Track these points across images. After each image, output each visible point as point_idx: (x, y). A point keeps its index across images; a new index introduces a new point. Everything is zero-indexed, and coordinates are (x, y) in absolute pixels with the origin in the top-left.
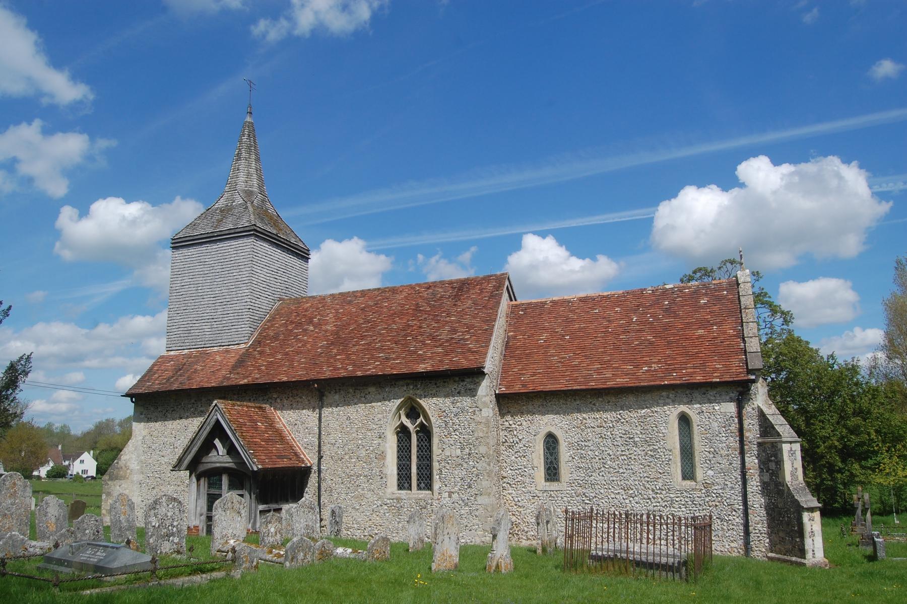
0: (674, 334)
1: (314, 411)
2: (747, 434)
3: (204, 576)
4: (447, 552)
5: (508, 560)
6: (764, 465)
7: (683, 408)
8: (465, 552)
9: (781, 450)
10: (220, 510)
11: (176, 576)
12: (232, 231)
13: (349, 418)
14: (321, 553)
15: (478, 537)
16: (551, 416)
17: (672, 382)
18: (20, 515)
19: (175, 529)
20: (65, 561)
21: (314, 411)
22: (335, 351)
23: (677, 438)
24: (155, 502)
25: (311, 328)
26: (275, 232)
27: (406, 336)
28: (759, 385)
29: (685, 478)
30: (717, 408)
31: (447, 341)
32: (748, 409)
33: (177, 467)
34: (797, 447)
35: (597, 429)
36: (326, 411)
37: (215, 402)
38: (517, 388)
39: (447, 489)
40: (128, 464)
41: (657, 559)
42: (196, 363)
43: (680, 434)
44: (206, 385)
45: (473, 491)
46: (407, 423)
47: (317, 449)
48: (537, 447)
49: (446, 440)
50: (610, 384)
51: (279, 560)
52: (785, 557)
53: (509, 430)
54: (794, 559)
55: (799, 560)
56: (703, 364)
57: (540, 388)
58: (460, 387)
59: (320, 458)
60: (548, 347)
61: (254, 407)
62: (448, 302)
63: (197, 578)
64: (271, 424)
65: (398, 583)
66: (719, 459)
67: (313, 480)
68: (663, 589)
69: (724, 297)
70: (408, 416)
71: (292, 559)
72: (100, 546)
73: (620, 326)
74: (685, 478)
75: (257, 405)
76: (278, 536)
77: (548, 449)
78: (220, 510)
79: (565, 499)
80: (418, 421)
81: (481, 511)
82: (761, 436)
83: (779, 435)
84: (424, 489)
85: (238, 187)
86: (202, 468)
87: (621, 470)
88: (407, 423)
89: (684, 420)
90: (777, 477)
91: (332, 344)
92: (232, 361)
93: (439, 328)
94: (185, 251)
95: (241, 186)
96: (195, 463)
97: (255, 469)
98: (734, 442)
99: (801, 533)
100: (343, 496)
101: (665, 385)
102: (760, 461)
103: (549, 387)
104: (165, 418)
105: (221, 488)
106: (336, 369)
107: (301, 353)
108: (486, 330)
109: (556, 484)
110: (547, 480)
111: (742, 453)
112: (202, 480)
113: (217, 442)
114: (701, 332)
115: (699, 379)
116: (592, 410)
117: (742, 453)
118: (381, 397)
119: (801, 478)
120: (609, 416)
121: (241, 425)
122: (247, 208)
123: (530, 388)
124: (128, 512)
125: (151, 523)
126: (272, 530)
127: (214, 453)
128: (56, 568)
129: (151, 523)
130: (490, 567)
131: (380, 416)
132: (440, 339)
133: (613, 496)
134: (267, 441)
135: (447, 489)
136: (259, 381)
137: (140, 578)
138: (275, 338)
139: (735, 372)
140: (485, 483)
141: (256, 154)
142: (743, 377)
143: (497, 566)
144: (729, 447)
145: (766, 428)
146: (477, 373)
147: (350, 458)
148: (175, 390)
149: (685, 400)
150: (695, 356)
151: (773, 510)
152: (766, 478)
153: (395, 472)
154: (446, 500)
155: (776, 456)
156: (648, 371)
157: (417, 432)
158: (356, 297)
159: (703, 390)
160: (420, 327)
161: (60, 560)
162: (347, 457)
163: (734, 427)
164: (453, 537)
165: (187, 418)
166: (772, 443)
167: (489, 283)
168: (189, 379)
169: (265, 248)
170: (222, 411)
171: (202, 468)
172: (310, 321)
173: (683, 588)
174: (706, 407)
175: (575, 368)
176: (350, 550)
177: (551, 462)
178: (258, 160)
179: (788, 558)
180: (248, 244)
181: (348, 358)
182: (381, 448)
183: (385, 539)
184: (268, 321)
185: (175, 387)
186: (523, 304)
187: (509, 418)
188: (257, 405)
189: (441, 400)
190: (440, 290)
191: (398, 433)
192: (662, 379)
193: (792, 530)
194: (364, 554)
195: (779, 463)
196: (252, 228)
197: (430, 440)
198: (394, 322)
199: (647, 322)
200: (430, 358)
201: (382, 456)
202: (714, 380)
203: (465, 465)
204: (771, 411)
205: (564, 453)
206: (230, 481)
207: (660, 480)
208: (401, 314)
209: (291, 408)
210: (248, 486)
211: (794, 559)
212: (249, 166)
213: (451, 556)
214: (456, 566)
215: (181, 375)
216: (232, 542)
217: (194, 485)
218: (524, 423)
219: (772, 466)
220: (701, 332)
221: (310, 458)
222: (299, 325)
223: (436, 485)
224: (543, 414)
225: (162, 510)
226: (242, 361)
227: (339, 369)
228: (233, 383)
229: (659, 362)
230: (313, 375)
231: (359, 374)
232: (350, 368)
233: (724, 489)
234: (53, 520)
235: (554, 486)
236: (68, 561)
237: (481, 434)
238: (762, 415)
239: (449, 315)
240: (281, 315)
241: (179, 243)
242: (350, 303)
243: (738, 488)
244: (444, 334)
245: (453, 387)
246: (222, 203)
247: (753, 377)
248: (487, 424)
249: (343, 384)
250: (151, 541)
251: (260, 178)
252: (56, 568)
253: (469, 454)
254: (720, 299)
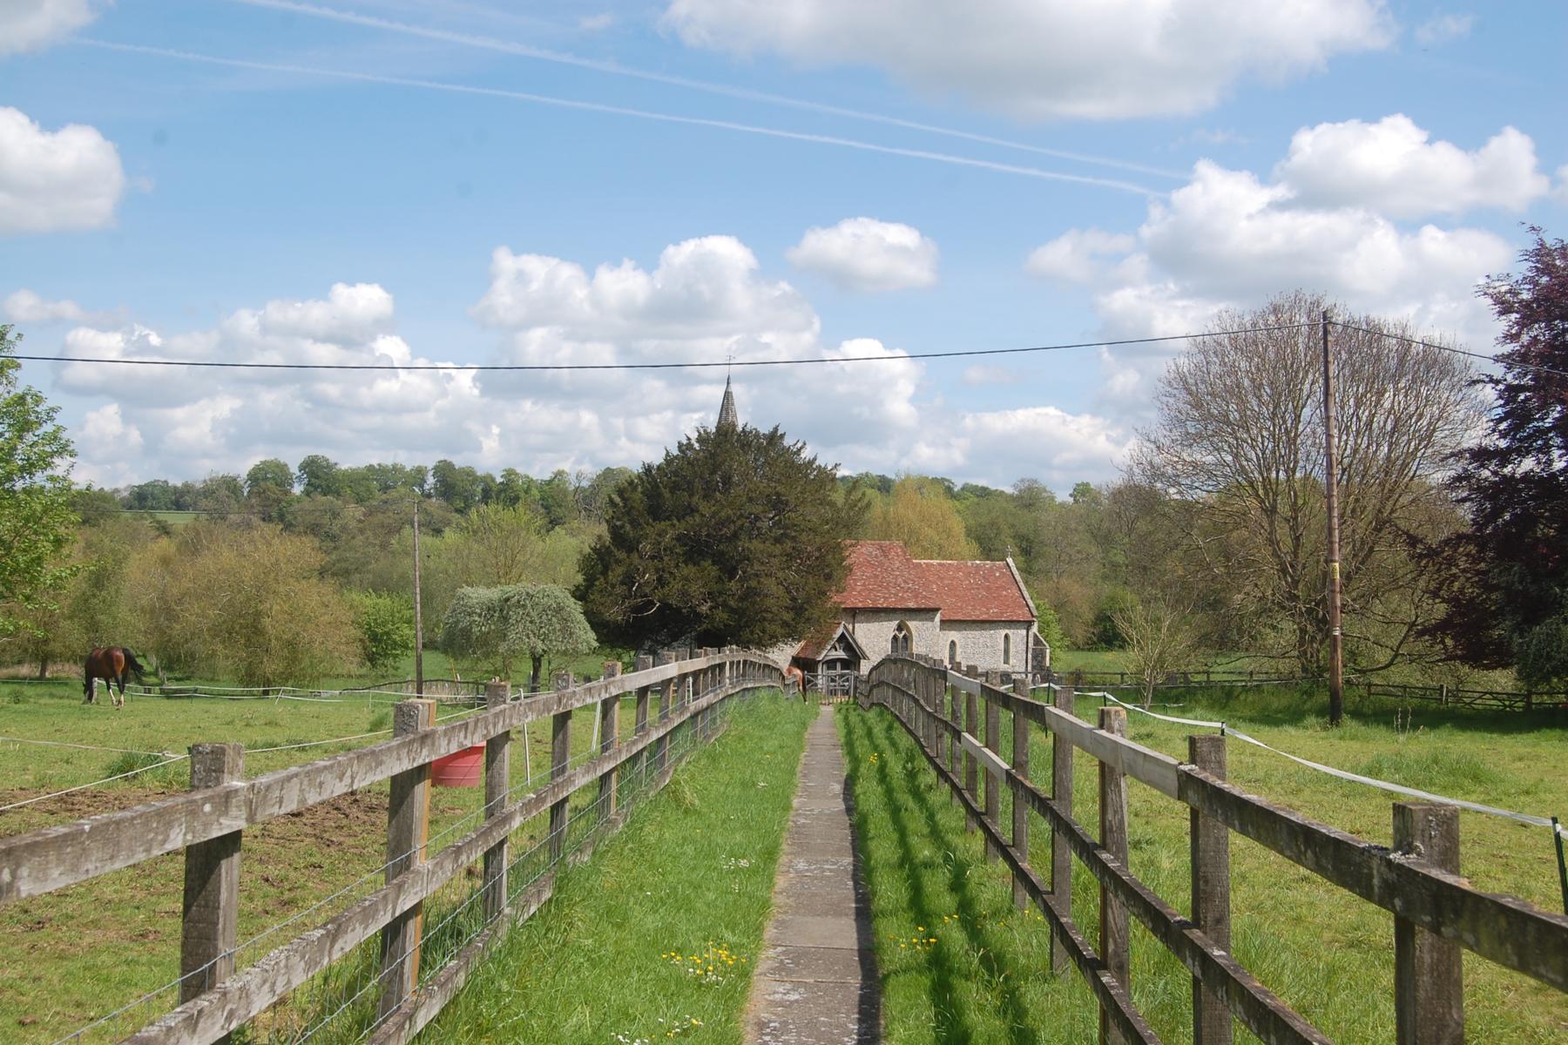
6: (1034, 658)
139: (1028, 617)
146: (937, 610)
156: (993, 613)
195: (1044, 658)
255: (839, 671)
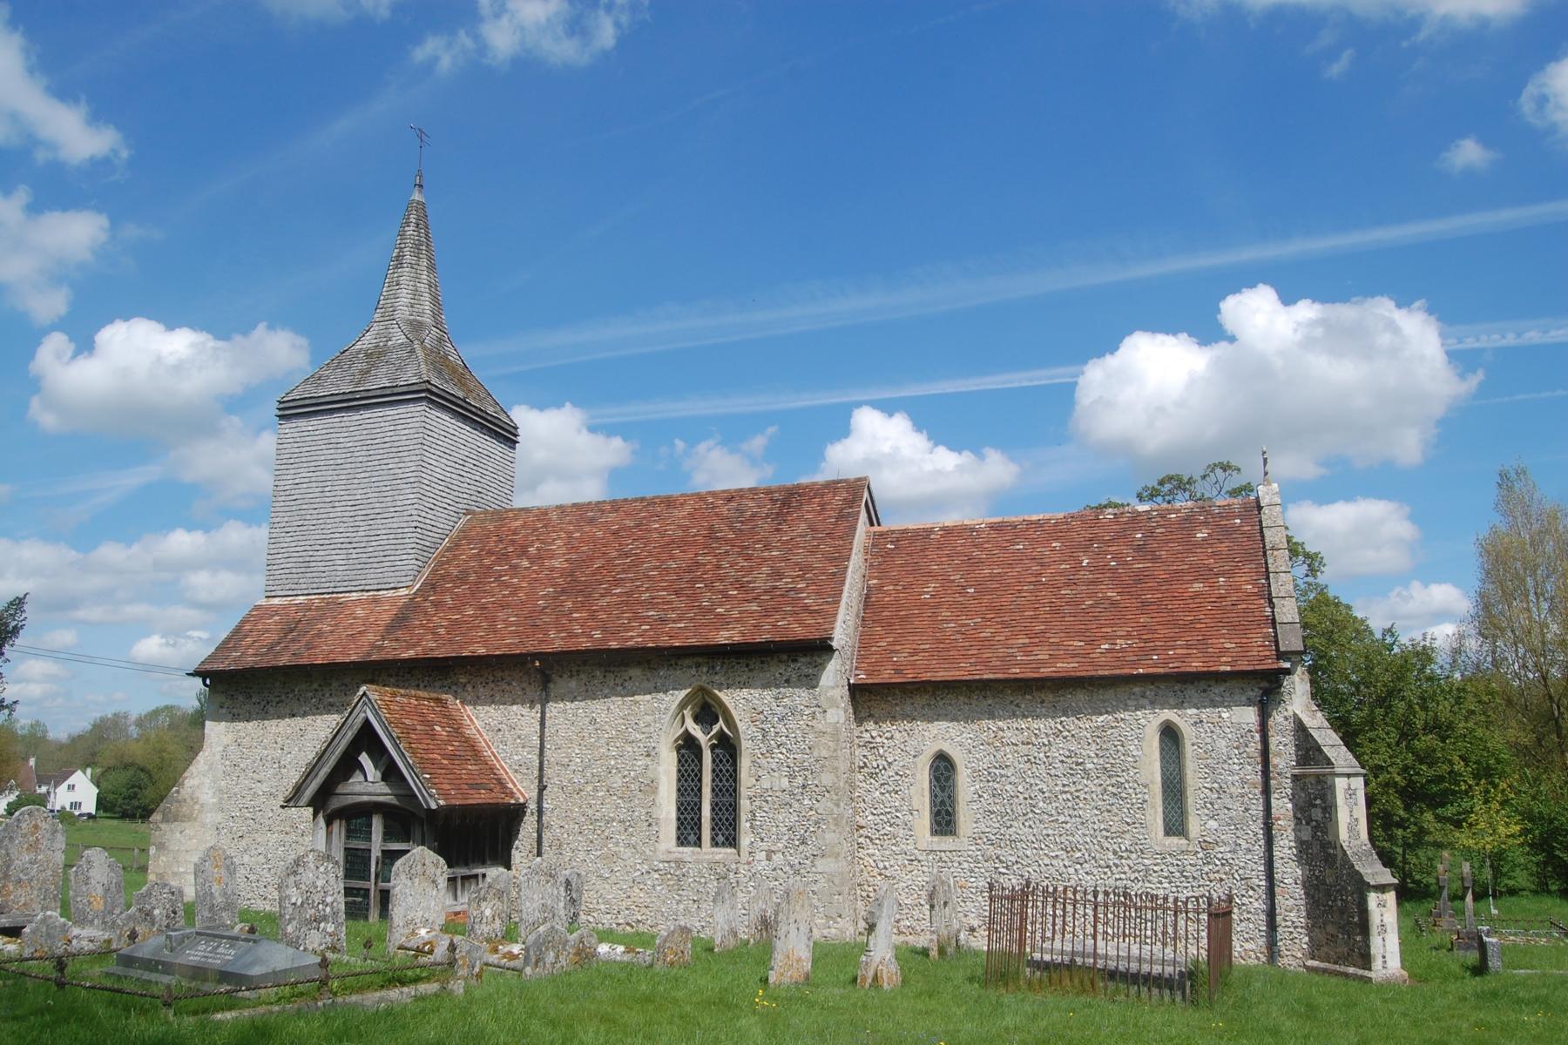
0: (1151, 589)
1: (531, 708)
2: (1274, 760)
3: (405, 989)
4: (793, 953)
5: (894, 967)
7: (1168, 714)
8: (824, 953)
9: (1332, 788)
10: (403, 877)
11: (360, 990)
12: (388, 391)
13: (593, 721)
14: (578, 954)
15: (846, 929)
16: (944, 724)
17: (1151, 670)
18: (44, 881)
19: (328, 909)
20: (158, 962)
21: (531, 708)
22: (569, 604)
23: (1158, 764)
24: (297, 862)
25: (526, 563)
26: (461, 394)
27: (693, 581)
28: (1296, 678)
29: (1168, 832)
30: (1225, 715)
31: (766, 592)
32: (1278, 719)
33: (292, 800)
34: (1358, 783)
35: (1021, 748)
36: (553, 708)
37: (363, 688)
38: (887, 675)
39: (764, 846)
40: (198, 794)
41: (1146, 968)
42: (321, 618)
43: (1163, 758)
44: (340, 659)
45: (809, 850)
46: (696, 731)
47: (536, 773)
48: (918, 776)
49: (763, 761)
50: (1046, 671)
51: (512, 964)
52: (1337, 967)
53: (871, 745)
54: (1351, 970)
55: (1360, 972)
56: (1203, 642)
57: (927, 676)
58: (791, 670)
59: (542, 789)
60: (939, 605)
61: (429, 699)
62: (765, 526)
63: (394, 994)
64: (457, 729)
65: (723, 1003)
66: (1228, 801)
67: (528, 827)
68: (1165, 1018)
69: (1236, 529)
70: (697, 719)
71: (537, 962)
72: (223, 937)
73: (1061, 573)
74: (1168, 832)
75: (434, 695)
76: (498, 921)
77: (937, 779)
78: (403, 877)
79: (965, 865)
80: (716, 728)
81: (822, 883)
82: (1299, 764)
83: (1329, 762)
84: (723, 845)
85: (398, 314)
86: (335, 803)
87: (1062, 819)
88: (696, 731)
89: (1170, 734)
91: (563, 591)
92: (386, 618)
93: (751, 570)
94: (302, 423)
95: (403, 312)
96: (324, 794)
97: (434, 806)
98: (1253, 774)
99: (1364, 927)
100: (582, 855)
101: (1139, 676)
102: (1295, 805)
103: (942, 675)
104: (264, 714)
105: (370, 839)
106: (572, 635)
107: (508, 606)
108: (834, 574)
109: (950, 839)
110: (934, 833)
111: (1266, 791)
112: (336, 825)
113: (364, 759)
114: (1198, 586)
115: (1196, 665)
116: (1014, 715)
117: (1266, 791)
118: (651, 685)
119: (1364, 835)
120: (1043, 725)
121: (408, 730)
122: (413, 351)
123: (909, 676)
124: (225, 879)
125: (288, 897)
126: (488, 912)
127: (357, 777)
128: (146, 976)
129: (288, 897)
130: (864, 979)
131: (648, 718)
132: (754, 589)
133: (1047, 861)
134: (452, 757)
135: (764, 846)
136: (436, 654)
137: (302, 994)
138: (462, 579)
139: (1257, 655)
140: (829, 836)
141: (429, 259)
142: (1270, 664)
143: (875, 978)
144: (1244, 782)
145: (1307, 750)
146: (820, 649)
147: (595, 789)
148: (285, 667)
149: (1172, 701)
150: (1188, 627)
151: (1316, 887)
152: (1306, 835)
153: (673, 815)
154: (761, 864)
155: (1323, 797)
156: (1111, 650)
157: (713, 747)
158: (603, 511)
159: (1203, 685)
160: (719, 567)
161: (150, 961)
162: (589, 788)
163: (1254, 747)
164: (804, 928)
165: (304, 715)
166: (1318, 776)
167: (835, 494)
168: (309, 646)
169: (444, 422)
170: (375, 704)
171: (335, 803)
172: (523, 552)
173: (1195, 1017)
174: (1206, 713)
175: (986, 643)
176: (621, 949)
177: (942, 803)
178: (432, 268)
179: (1342, 969)
180: (417, 412)
181: (593, 616)
182: (650, 774)
183: (685, 930)
184: (448, 549)
185: (284, 660)
186: (893, 532)
187: (870, 725)
188: (434, 695)
189: (756, 692)
190: (751, 504)
191: (678, 749)
192: (1134, 664)
193: (1349, 923)
194: (646, 955)
195: (1329, 809)
196: (424, 386)
197: (734, 764)
198: (672, 557)
199: (1104, 568)
200: (738, 620)
201: (651, 787)
202: (1223, 668)
203: (796, 805)
204: (1316, 722)
205: (965, 786)
206: (385, 827)
207: (1127, 836)
208: (684, 543)
209: (492, 701)
210: (418, 836)
211: (1351, 970)
212: (417, 278)
213: (799, 960)
214: (807, 977)
215: (293, 641)
216: (423, 932)
217: (322, 833)
218: (897, 735)
219: (1317, 814)
220: (1198, 586)
221: (523, 789)
222: (503, 557)
223: (745, 840)
224: (930, 720)
225: (308, 876)
226: (401, 620)
227: (577, 636)
228: (390, 657)
229: (1128, 636)
230: (531, 646)
231: (614, 645)
232: (597, 635)
233: (1234, 852)
234: (100, 891)
235: (947, 843)
236: (163, 963)
237: (824, 753)
238: (1300, 729)
239: (767, 547)
240: (470, 540)
241: (291, 410)
242: (591, 521)
243: (1259, 850)
244: (761, 580)
245: (777, 670)
246: (368, 341)
247: (1287, 665)
248: (835, 736)
249: (585, 663)
250: (290, 929)
251: (435, 300)
252: (146, 976)
253: (804, 787)
254: (1229, 532)
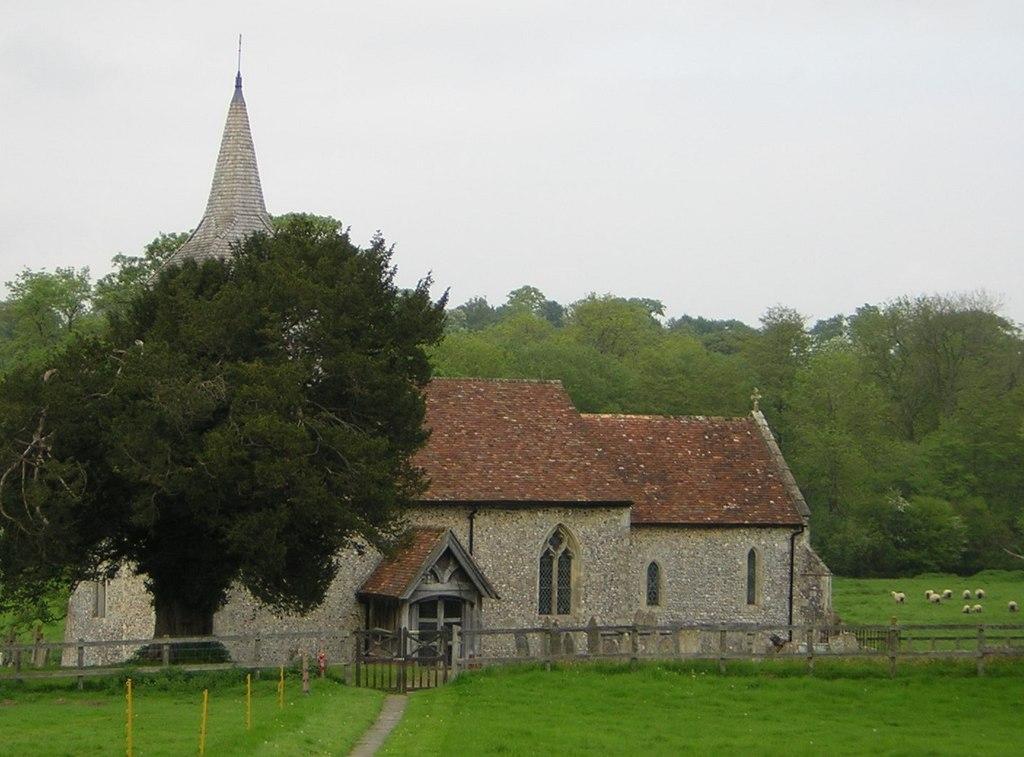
13: (499, 543)
90: (818, 602)
110: (648, 604)
255: (441, 620)
